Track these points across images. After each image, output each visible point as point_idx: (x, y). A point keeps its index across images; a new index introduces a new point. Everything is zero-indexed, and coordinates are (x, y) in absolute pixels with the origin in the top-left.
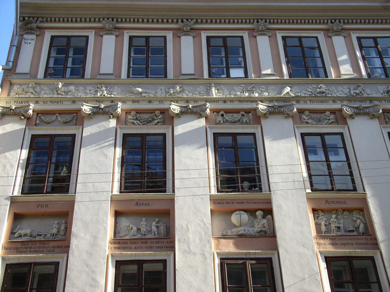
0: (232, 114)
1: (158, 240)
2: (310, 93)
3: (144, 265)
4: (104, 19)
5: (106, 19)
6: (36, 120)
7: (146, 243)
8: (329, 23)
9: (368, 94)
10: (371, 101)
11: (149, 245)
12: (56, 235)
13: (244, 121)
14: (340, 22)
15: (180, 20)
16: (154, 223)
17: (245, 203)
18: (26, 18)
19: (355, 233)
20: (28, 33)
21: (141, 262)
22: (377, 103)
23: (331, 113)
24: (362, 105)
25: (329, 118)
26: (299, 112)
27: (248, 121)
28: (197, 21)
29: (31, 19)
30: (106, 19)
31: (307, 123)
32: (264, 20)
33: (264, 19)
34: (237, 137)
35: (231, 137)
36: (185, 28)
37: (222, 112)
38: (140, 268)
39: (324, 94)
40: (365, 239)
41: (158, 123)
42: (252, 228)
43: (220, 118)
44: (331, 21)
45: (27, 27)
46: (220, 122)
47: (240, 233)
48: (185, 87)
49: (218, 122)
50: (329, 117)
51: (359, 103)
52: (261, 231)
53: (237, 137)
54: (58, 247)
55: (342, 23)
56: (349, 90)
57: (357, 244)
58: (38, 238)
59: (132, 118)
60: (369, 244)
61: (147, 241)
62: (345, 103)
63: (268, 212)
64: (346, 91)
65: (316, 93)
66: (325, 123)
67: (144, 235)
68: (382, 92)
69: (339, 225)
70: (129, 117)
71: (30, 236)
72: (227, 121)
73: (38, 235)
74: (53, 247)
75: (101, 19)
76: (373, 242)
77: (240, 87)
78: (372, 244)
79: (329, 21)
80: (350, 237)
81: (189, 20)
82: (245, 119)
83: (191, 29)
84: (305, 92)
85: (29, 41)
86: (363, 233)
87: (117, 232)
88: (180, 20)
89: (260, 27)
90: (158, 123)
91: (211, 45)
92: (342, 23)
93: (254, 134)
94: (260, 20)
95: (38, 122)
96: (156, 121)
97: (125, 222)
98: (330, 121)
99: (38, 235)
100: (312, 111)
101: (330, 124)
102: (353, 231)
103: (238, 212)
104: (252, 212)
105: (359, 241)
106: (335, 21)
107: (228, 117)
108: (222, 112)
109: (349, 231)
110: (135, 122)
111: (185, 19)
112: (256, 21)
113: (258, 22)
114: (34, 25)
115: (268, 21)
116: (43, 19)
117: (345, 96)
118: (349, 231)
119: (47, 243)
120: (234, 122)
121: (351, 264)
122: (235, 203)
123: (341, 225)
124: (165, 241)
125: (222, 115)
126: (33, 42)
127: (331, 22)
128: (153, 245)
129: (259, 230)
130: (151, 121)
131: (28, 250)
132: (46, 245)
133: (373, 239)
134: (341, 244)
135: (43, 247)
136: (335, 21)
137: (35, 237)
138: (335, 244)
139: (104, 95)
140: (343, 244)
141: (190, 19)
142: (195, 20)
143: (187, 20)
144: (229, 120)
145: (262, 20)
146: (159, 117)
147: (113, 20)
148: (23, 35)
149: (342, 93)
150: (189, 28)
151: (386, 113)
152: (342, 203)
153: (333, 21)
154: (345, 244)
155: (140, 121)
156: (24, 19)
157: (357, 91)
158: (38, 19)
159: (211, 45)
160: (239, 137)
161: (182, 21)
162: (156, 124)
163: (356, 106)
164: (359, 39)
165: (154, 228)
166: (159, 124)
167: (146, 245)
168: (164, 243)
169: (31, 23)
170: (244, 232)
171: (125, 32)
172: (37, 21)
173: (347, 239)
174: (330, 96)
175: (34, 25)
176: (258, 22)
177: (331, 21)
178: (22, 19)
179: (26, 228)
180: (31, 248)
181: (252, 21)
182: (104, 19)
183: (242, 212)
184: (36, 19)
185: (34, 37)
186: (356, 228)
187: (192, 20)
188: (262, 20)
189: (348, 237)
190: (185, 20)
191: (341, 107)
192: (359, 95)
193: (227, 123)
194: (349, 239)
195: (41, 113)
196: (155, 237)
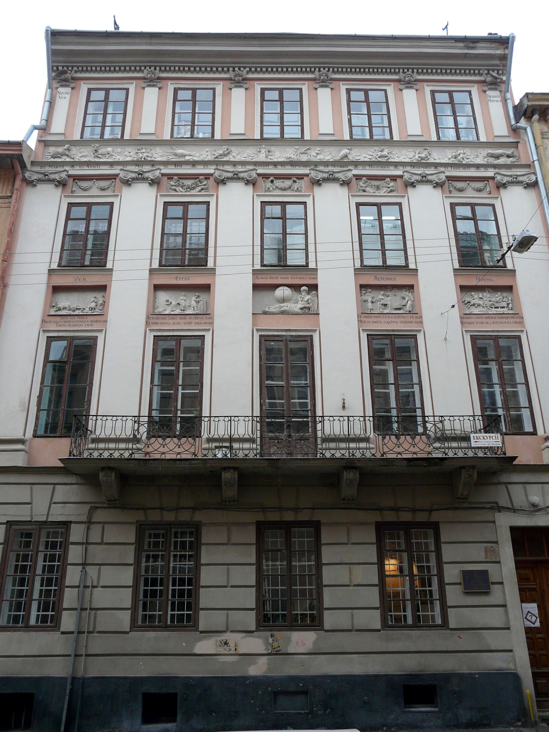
0: (282, 180)
1: (196, 316)
2: (370, 157)
3: (183, 341)
4: (145, 68)
5: (148, 68)
6: (72, 187)
7: (185, 318)
8: (401, 73)
9: (435, 159)
10: (436, 167)
11: (188, 321)
12: (95, 309)
13: (296, 188)
14: (413, 72)
15: (231, 69)
16: (194, 298)
17: (290, 278)
18: (60, 68)
20: (62, 86)
21: (179, 338)
22: (442, 169)
23: (391, 180)
24: (426, 172)
25: (389, 186)
26: (356, 179)
27: (299, 188)
28: (250, 70)
29: (65, 68)
30: (148, 68)
31: (364, 191)
32: (327, 69)
33: (327, 67)
34: (287, 206)
35: (280, 206)
36: (236, 79)
37: (271, 178)
38: (179, 344)
39: (386, 158)
41: (202, 189)
42: (295, 305)
43: (269, 184)
44: (403, 71)
45: (60, 78)
46: (269, 188)
47: (283, 309)
48: (233, 149)
49: (267, 189)
50: (388, 184)
51: (422, 169)
52: (305, 307)
53: (287, 206)
54: (97, 321)
55: (415, 73)
56: (414, 154)
57: (402, 322)
58: (77, 312)
59: (174, 184)
61: (186, 316)
62: (408, 168)
63: (313, 287)
64: (411, 154)
65: (377, 157)
66: (384, 191)
67: (184, 310)
68: (450, 157)
69: (385, 303)
70: (172, 183)
71: (69, 310)
72: (277, 187)
73: (77, 309)
74: (91, 321)
75: (143, 68)
76: (418, 320)
77: (293, 149)
79: (401, 70)
80: (395, 315)
81: (242, 69)
82: (296, 186)
83: (245, 79)
84: (365, 155)
85: (64, 95)
86: (410, 312)
87: (156, 307)
88: (231, 69)
89: (322, 77)
90: (202, 189)
91: (266, 99)
92: (415, 73)
93: (305, 203)
94: (322, 69)
95: (74, 189)
96: (200, 188)
97: (163, 296)
98: (389, 189)
99: (77, 309)
100: (371, 178)
101: (389, 193)
102: (400, 309)
103: (281, 288)
104: (296, 288)
105: (403, 320)
106: (408, 71)
107: (279, 183)
108: (271, 178)
109: (396, 309)
110: (177, 189)
111: (237, 67)
112: (317, 69)
113: (319, 71)
114: (68, 76)
115: (331, 69)
116: (78, 68)
117: (409, 161)
118: (396, 309)
119: (85, 317)
120: (285, 189)
121: (392, 343)
122: (279, 278)
123: (388, 303)
124: (204, 317)
125: (272, 182)
126: (68, 97)
127: (403, 72)
128: (191, 321)
129: (303, 306)
130: (194, 188)
131: (67, 324)
132: (85, 320)
135: (81, 322)
136: (408, 71)
137: (74, 311)
139: (144, 159)
141: (242, 67)
142: (248, 69)
143: (239, 69)
144: (279, 187)
145: (324, 69)
146: (203, 184)
147: (155, 69)
148: (57, 88)
149: (406, 157)
150: (240, 78)
151: (451, 180)
153: (406, 70)
155: (182, 187)
156: (58, 69)
157: (423, 155)
158: (72, 69)
159: (266, 99)
160: (288, 207)
161: (234, 70)
162: (200, 191)
163: (419, 172)
164: (433, 92)
165: (193, 303)
166: (203, 191)
167: (184, 321)
168: (202, 318)
169: (65, 72)
170: (287, 308)
171: (169, 83)
172: (71, 71)
173: (392, 317)
174: (393, 160)
175: (68, 76)
176: (319, 71)
177: (403, 71)
178: (55, 68)
179: (66, 301)
180: (70, 322)
181: (313, 69)
182: (145, 68)
183: (286, 288)
184: (70, 68)
185: (69, 90)
187: (245, 68)
188: (324, 69)
189: (393, 315)
190: (237, 69)
191: (402, 174)
192: (424, 159)
193: (277, 190)
195: (77, 179)
196: (194, 313)
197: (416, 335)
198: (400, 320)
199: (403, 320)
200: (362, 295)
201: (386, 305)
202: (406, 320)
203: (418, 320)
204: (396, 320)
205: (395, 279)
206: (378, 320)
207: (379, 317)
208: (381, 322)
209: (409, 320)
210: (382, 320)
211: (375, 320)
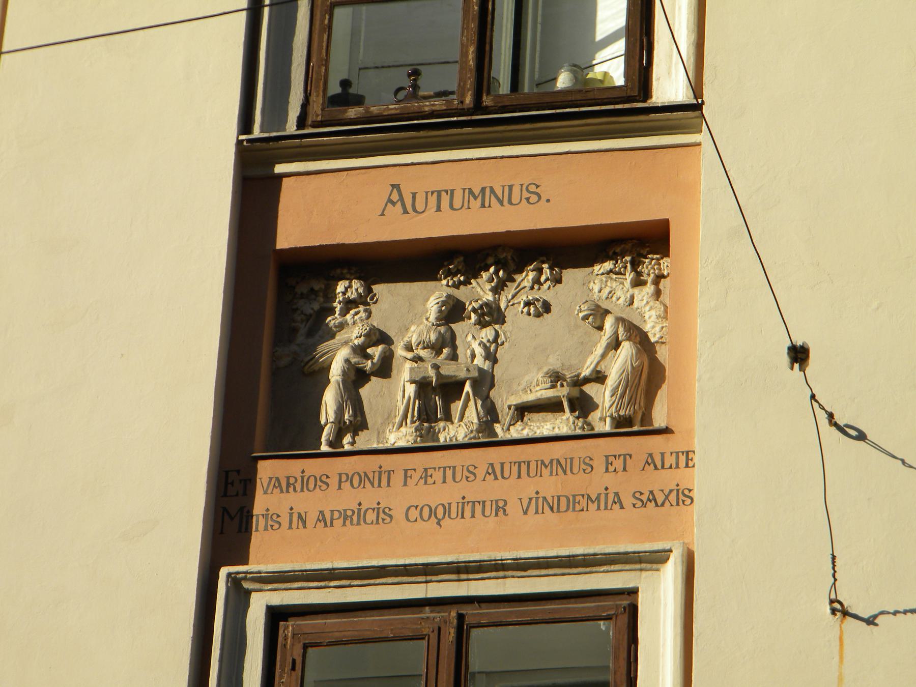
19: (562, 423)
40: (608, 464)
60: (627, 500)
78: (653, 498)
102: (552, 407)
105: (550, 485)
109: (522, 411)
133: (670, 460)
134: (414, 514)
138: (371, 516)
140: (433, 512)
152: (506, 198)
154: (447, 510)
173: (471, 473)
186: (579, 382)
194: (491, 471)
197: (633, 592)
198: (528, 487)
199: (550, 485)
200: (295, 331)
201: (451, 389)
202: (575, 483)
203: (663, 480)
204: (491, 490)
205: (533, 194)
206: (369, 497)
207: (383, 477)
208: (383, 514)
209: (598, 482)
210: (397, 497)
211: (347, 499)
